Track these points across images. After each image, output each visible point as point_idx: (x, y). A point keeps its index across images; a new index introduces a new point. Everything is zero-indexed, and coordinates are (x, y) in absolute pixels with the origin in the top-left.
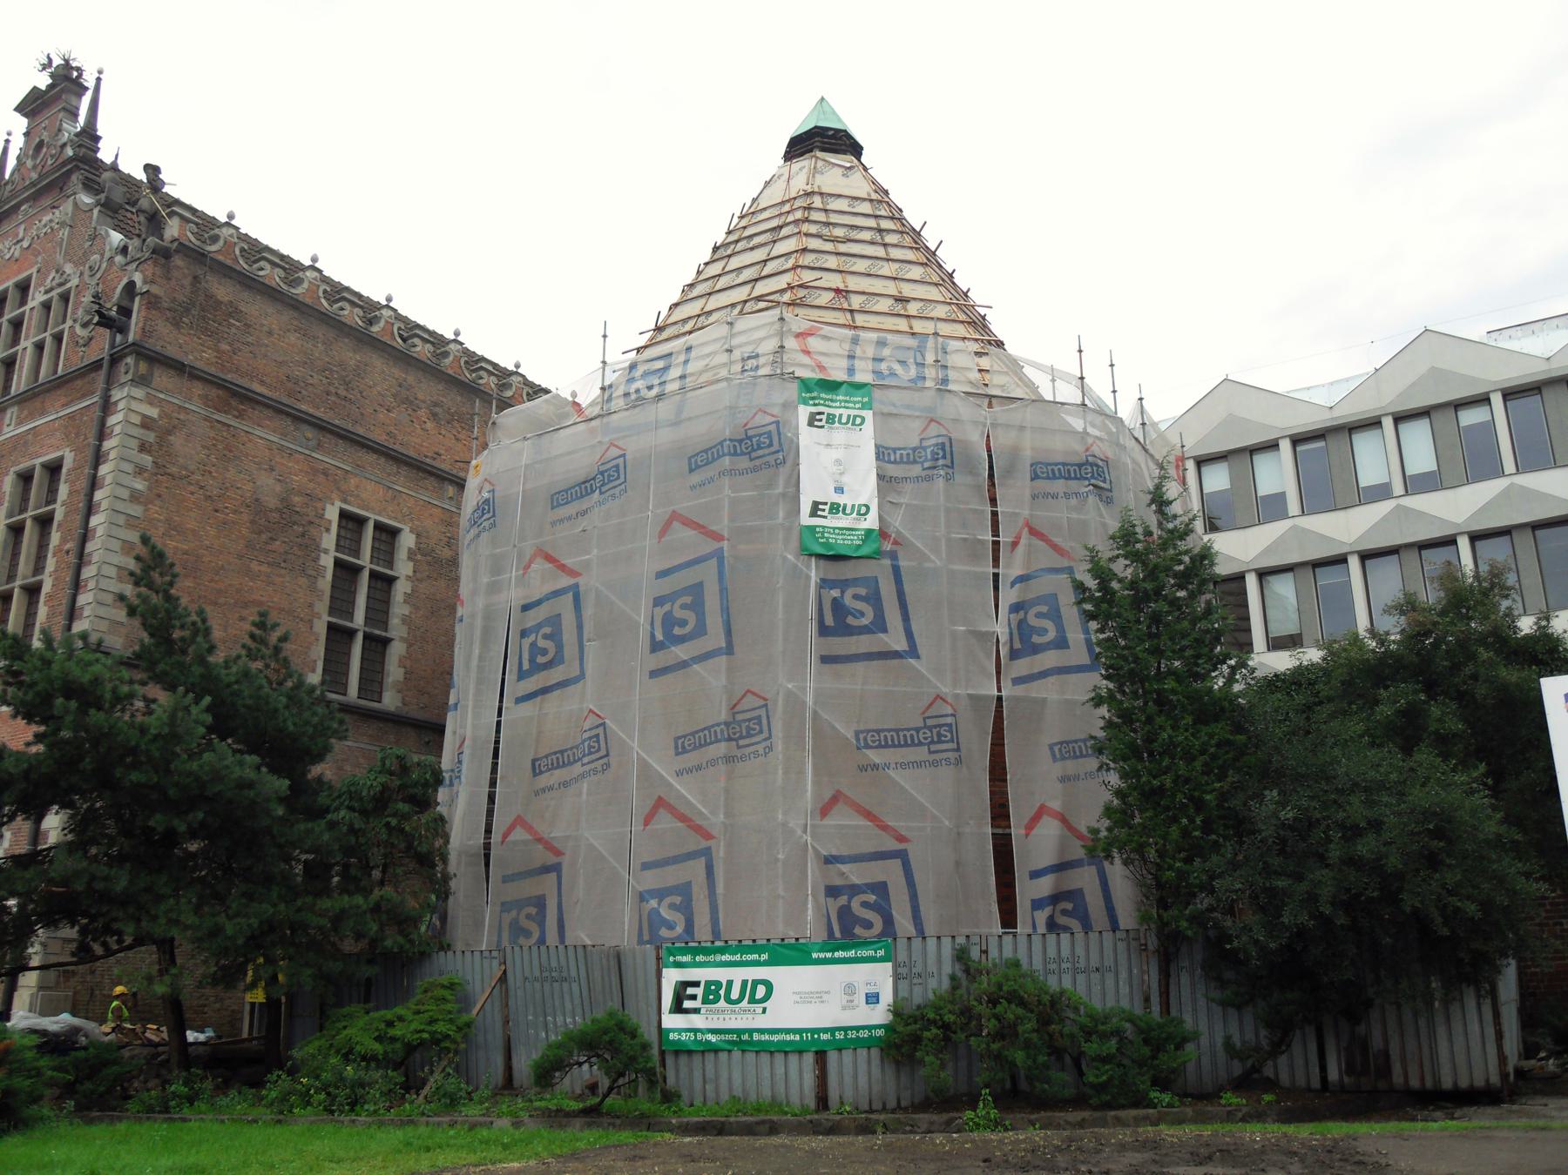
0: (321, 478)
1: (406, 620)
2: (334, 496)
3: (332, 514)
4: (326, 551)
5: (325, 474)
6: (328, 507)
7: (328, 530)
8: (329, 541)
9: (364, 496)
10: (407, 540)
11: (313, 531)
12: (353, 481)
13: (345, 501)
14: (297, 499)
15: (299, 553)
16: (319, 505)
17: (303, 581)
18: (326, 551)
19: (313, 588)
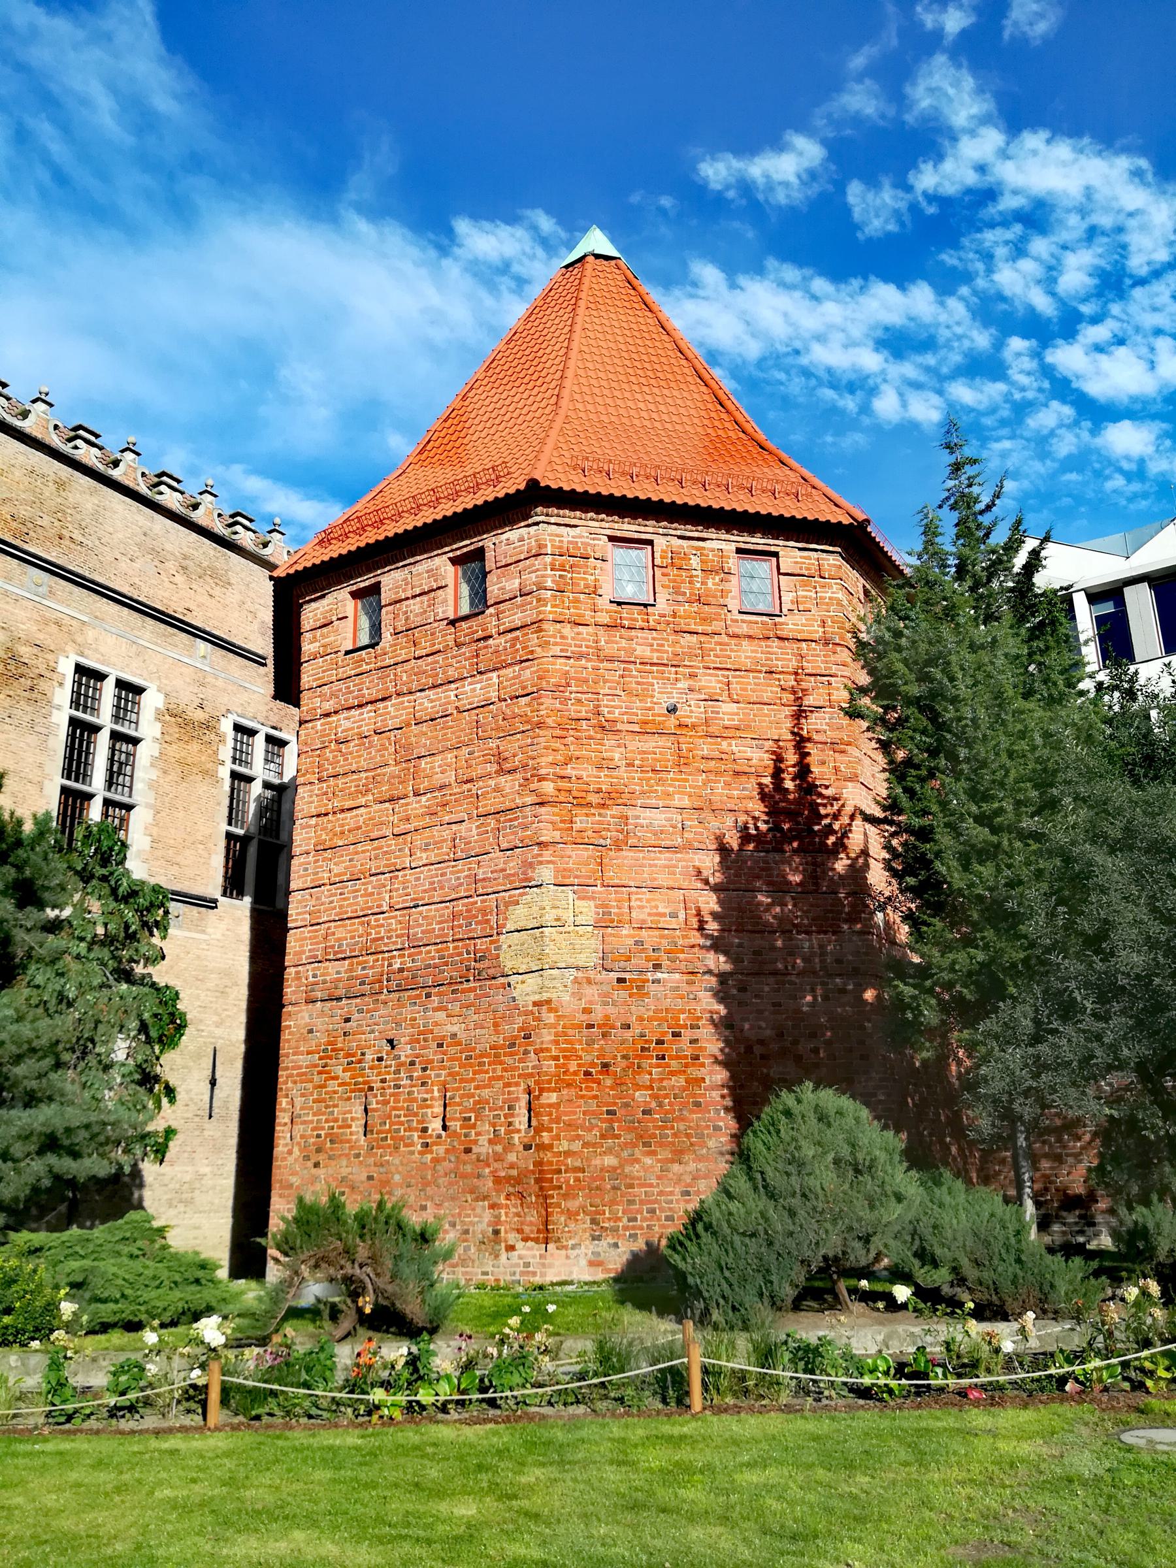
0: (53, 628)
1: (152, 785)
2: (68, 648)
3: (67, 668)
4: (59, 708)
5: (58, 624)
6: (62, 660)
7: (61, 684)
8: (63, 696)
9: (102, 649)
10: (151, 701)
11: (43, 685)
12: (91, 634)
13: (82, 654)
14: (25, 651)
15: (29, 709)
16: (50, 656)
17: (32, 739)
18: (59, 708)
19: (43, 748)
